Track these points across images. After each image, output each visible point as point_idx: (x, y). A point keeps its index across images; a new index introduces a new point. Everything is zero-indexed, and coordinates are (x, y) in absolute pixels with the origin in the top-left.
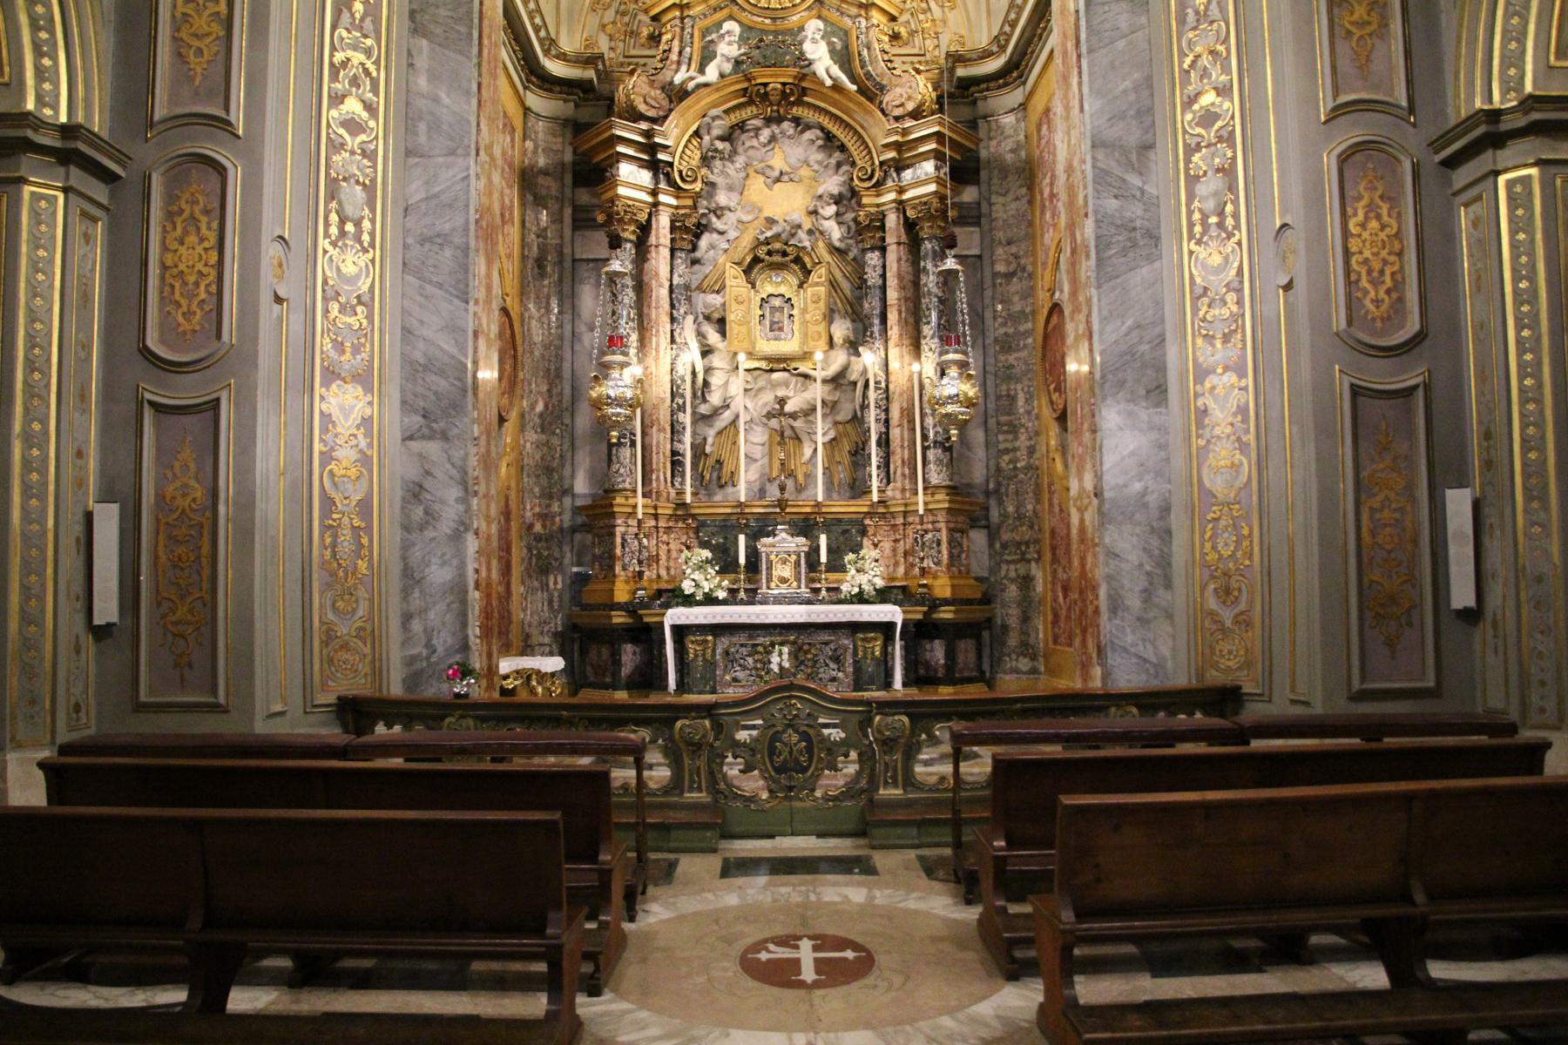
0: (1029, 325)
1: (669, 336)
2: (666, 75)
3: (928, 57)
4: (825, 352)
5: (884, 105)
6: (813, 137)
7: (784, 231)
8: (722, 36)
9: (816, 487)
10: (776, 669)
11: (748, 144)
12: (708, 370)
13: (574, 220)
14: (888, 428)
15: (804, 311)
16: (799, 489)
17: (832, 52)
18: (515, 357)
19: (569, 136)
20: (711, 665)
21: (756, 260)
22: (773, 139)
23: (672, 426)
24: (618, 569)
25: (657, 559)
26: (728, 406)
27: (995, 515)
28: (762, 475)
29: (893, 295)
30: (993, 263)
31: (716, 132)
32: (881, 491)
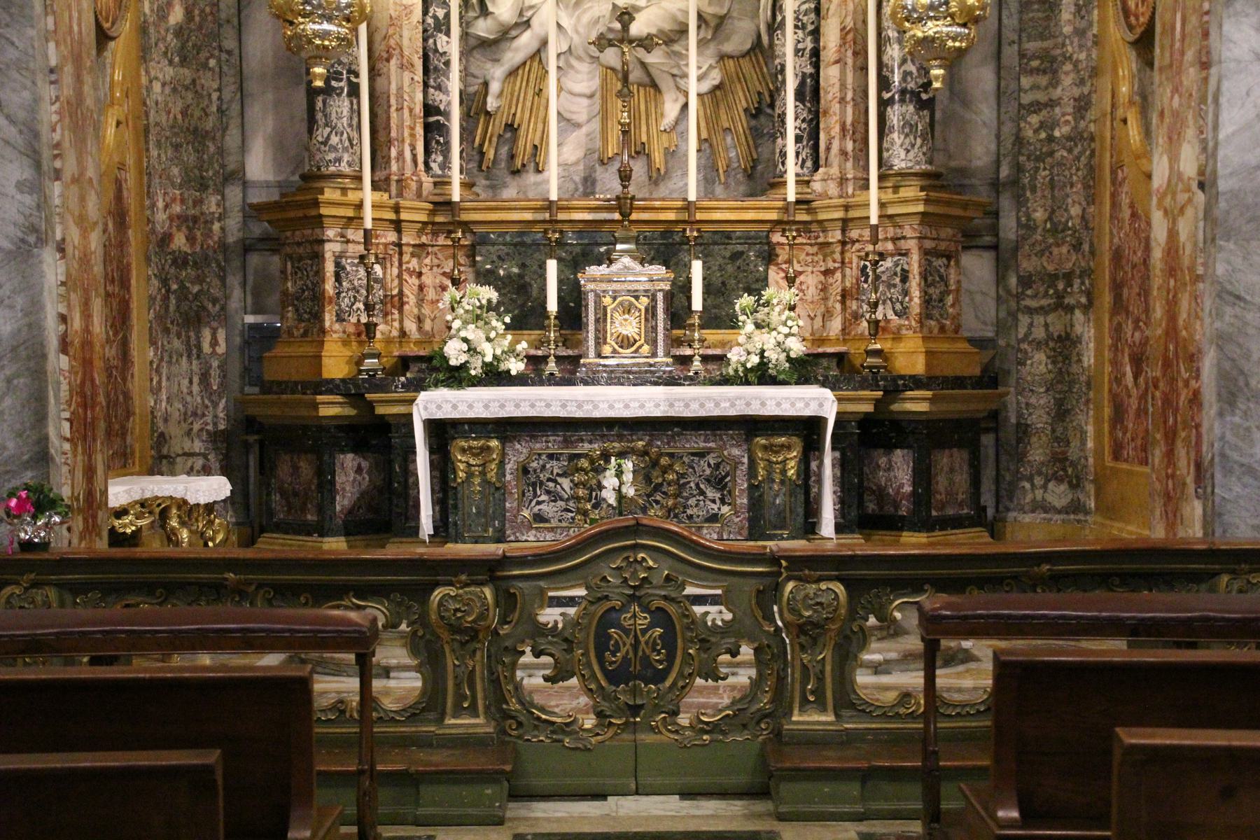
9: (685, 174)
10: (612, 500)
14: (816, 66)
16: (656, 178)
20: (497, 490)
23: (426, 58)
24: (329, 319)
27: (1009, 226)
28: (589, 152)
32: (802, 182)
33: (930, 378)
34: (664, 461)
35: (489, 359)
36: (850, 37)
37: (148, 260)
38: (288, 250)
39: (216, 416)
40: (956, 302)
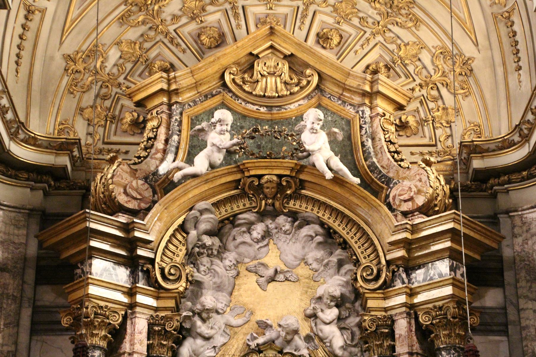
2: (151, 164)
3: (440, 147)
7: (278, 338)
11: (239, 239)
13: (33, 323)
17: (333, 142)
19: (34, 228)
22: (267, 234)
31: (203, 226)
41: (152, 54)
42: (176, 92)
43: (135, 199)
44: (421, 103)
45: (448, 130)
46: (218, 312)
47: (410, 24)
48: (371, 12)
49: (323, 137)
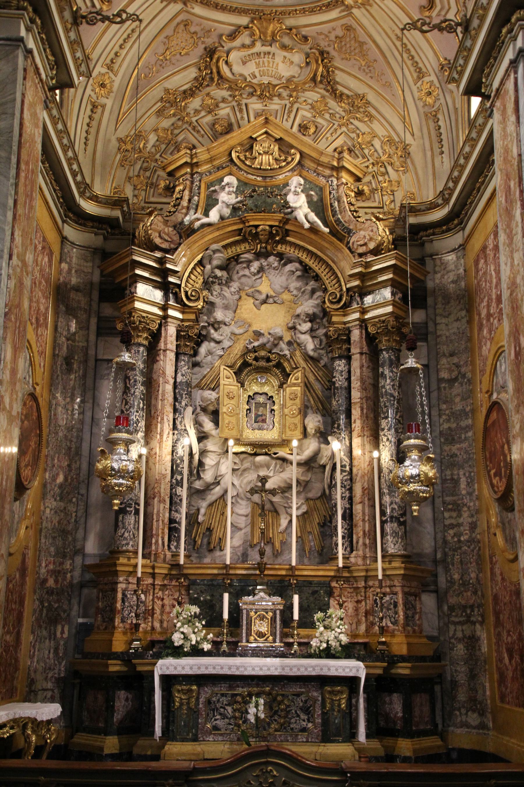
0: (470, 421)
1: (171, 423)
2: (179, 217)
3: (386, 209)
4: (299, 440)
5: (351, 244)
6: (293, 269)
8: (223, 188)
10: (253, 720)
11: (241, 273)
12: (203, 453)
13: (98, 328)
14: (351, 504)
15: (283, 406)
16: (276, 554)
17: (310, 203)
18: (40, 436)
19: (98, 262)
20: (194, 712)
21: (245, 364)
22: (261, 270)
24: (117, 621)
25: (152, 613)
26: (218, 483)
27: (442, 580)
28: (245, 542)
29: (356, 395)
30: (438, 371)
31: (215, 262)
33: (410, 657)
34: (279, 698)
35: (194, 642)
36: (366, 492)
37: (35, 592)
38: (101, 587)
39: (60, 670)
40: (420, 618)
41: (180, 138)
42: (197, 164)
43: (167, 241)
44: (373, 176)
45: (392, 197)
46: (225, 324)
47: (366, 119)
48: (338, 109)
49: (303, 198)
